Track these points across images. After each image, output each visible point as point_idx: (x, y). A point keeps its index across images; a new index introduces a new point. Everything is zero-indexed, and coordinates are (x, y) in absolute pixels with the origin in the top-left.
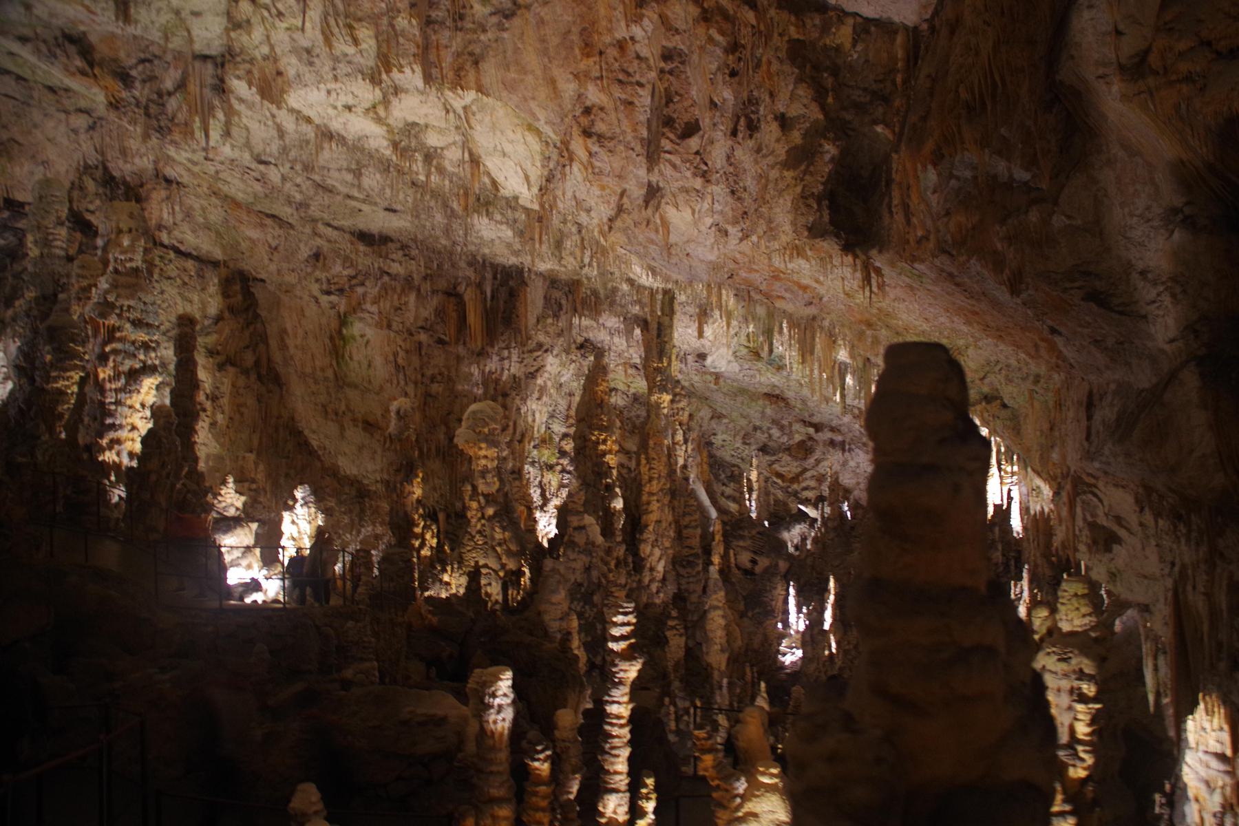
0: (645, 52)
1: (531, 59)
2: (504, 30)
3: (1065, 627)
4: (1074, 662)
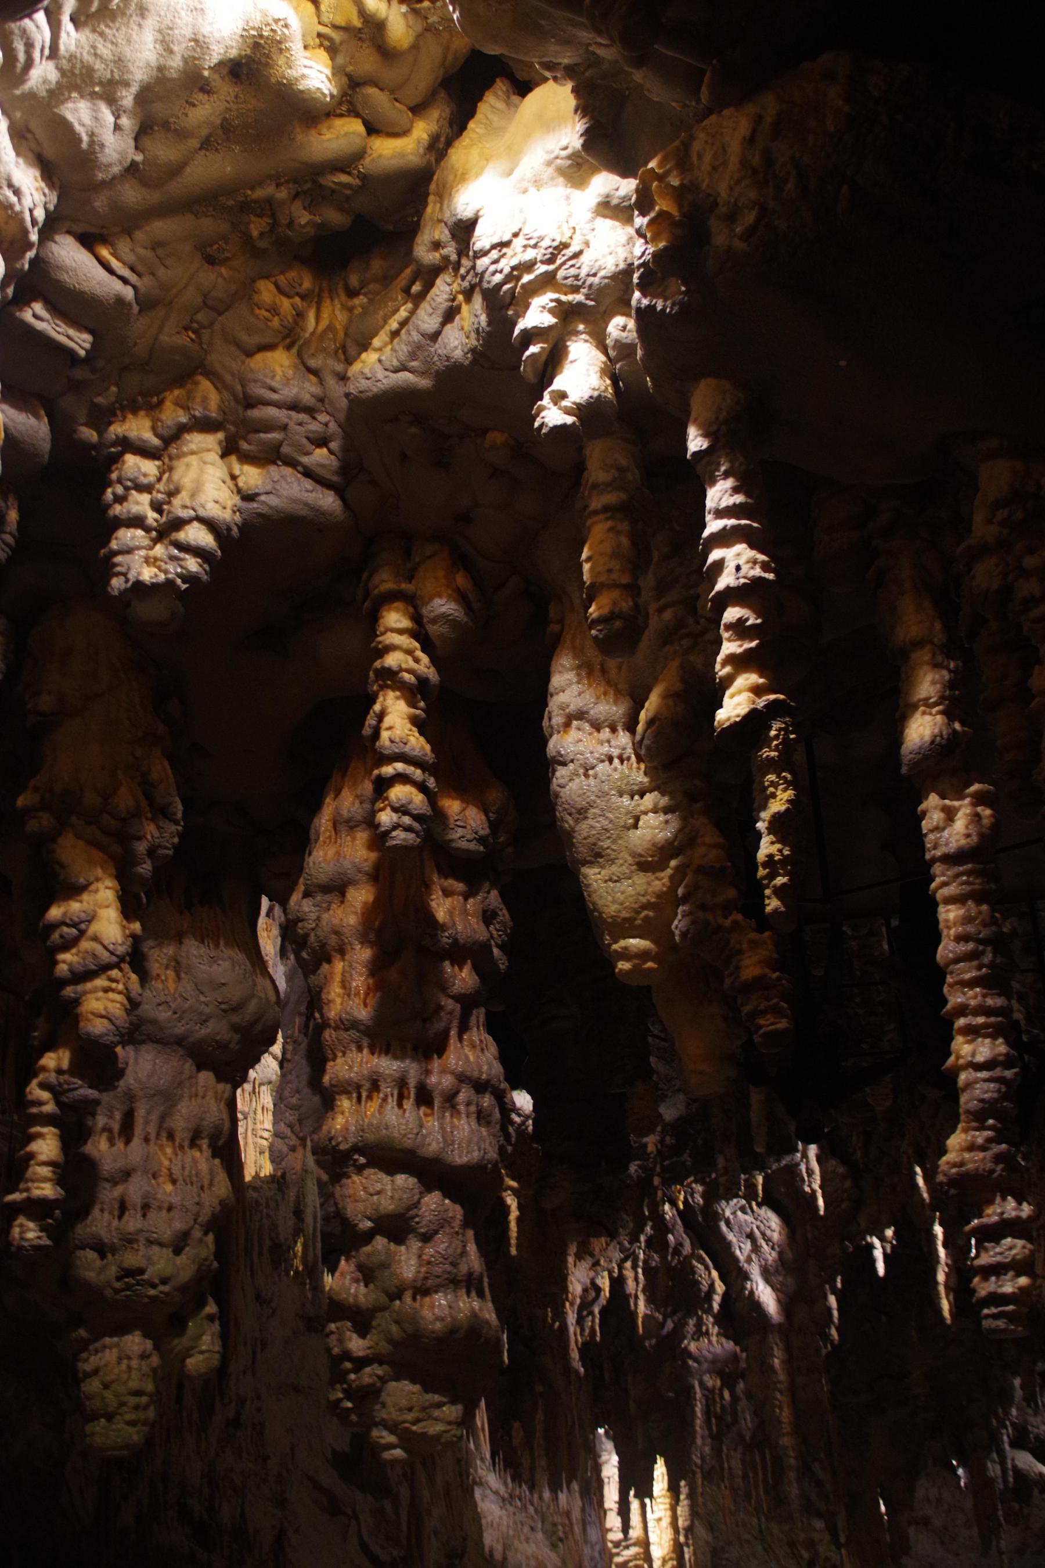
3: (135, 1342)
4: (113, 1271)
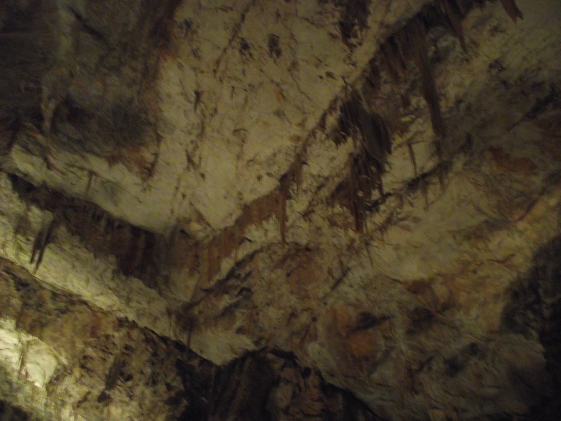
0: (117, 342)
1: (68, 331)
2: (59, 317)
